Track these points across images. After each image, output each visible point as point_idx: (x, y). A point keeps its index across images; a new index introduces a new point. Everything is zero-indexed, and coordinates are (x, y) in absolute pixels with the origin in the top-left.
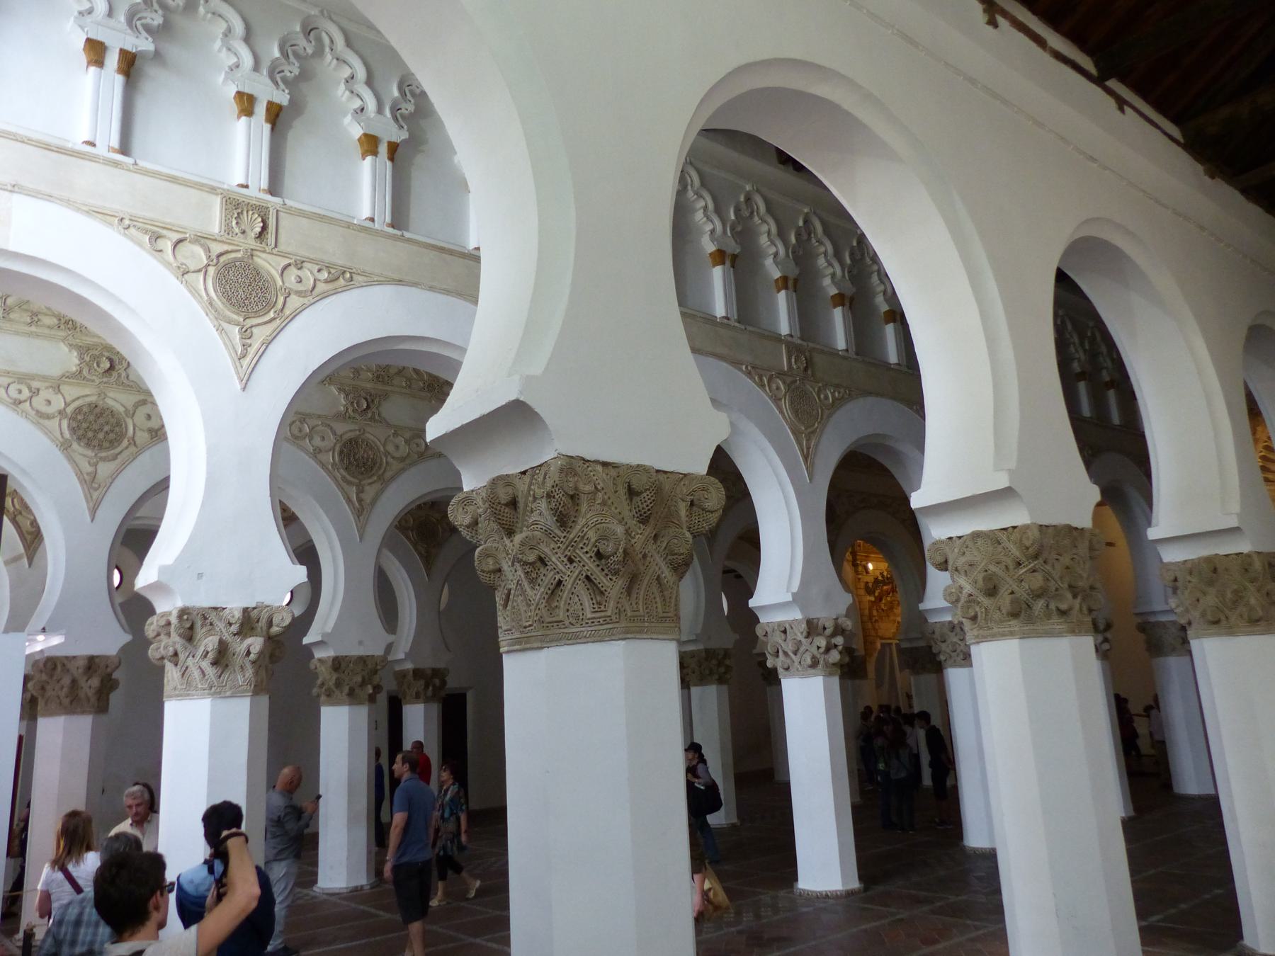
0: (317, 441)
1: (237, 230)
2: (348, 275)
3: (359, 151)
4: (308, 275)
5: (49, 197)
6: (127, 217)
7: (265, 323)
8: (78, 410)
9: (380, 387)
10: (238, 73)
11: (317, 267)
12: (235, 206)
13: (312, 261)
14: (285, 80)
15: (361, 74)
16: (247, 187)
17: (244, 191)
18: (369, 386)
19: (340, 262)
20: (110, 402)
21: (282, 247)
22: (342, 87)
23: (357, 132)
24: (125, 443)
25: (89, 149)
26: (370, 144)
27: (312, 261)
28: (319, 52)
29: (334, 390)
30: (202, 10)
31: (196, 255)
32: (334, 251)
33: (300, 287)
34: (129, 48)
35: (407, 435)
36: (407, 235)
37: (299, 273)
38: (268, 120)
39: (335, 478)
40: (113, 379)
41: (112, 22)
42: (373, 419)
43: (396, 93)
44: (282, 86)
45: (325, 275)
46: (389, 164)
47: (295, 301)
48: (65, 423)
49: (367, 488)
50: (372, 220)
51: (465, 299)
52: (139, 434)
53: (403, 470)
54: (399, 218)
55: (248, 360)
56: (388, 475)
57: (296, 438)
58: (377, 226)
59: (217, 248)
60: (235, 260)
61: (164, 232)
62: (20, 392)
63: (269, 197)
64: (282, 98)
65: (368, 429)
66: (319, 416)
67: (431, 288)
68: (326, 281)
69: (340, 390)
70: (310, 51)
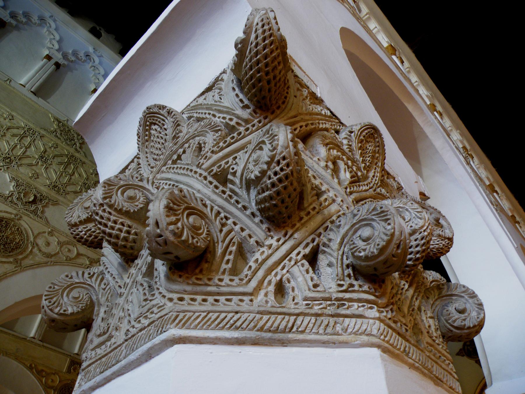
9: (53, 194)
18: (43, 189)
29: (7, 177)
42: (35, 212)
53: (46, 264)
56: (28, 262)
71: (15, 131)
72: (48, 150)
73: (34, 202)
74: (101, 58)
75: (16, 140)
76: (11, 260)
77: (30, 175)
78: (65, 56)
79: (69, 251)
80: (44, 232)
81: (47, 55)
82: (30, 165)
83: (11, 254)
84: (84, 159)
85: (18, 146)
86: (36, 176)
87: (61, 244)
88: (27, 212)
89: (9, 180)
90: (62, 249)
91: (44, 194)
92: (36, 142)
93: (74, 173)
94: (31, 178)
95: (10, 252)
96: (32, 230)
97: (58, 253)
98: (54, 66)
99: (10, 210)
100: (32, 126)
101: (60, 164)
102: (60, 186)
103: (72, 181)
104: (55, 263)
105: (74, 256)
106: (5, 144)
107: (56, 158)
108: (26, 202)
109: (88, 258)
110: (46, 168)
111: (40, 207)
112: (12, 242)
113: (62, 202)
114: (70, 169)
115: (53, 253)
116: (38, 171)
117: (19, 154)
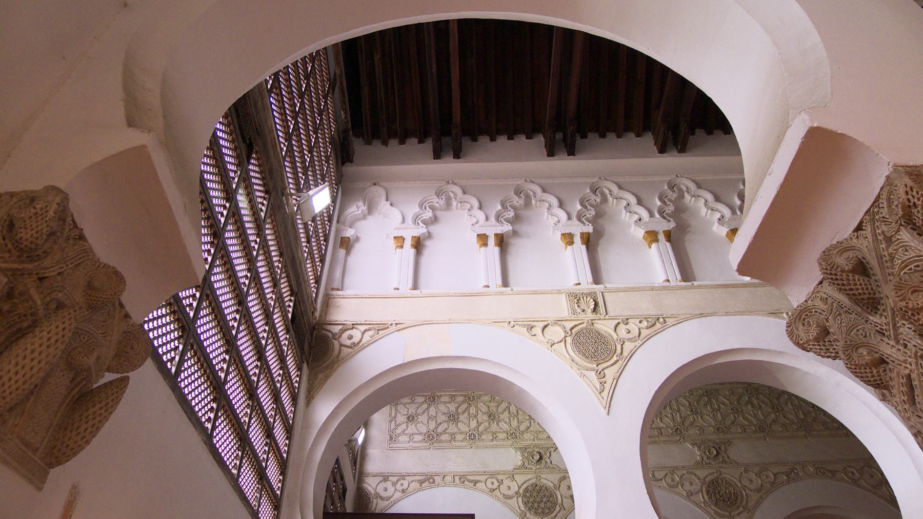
0: (687, 485)
1: (579, 311)
2: (661, 320)
3: (646, 244)
4: (633, 326)
5: (469, 321)
6: (512, 321)
7: (612, 365)
8: (526, 490)
9: (721, 436)
10: (560, 225)
11: (638, 321)
12: (576, 298)
13: (633, 317)
14: (587, 220)
15: (633, 200)
16: (579, 284)
17: (578, 287)
18: (713, 437)
19: (654, 313)
20: (543, 481)
21: (611, 313)
22: (624, 211)
23: (640, 233)
24: (558, 508)
25: (487, 289)
26: (652, 237)
27: (633, 317)
28: (604, 199)
30: (533, 202)
31: (556, 333)
32: (646, 306)
33: (630, 336)
34: (499, 232)
35: (756, 469)
36: (696, 283)
37: (627, 327)
38: (583, 243)
39: (708, 513)
40: (543, 465)
41: (488, 223)
42: (724, 462)
43: (659, 203)
44: (587, 223)
45: (645, 324)
46: (668, 244)
47: (628, 347)
48: (520, 499)
50: (668, 281)
51: (758, 315)
52: (564, 500)
54: (687, 274)
55: (608, 394)
56: (751, 504)
58: (672, 284)
59: (569, 325)
60: (582, 330)
61: (535, 324)
62: (493, 483)
63: (595, 286)
64: (589, 229)
65: (723, 470)
66: (683, 467)
67: (727, 314)
68: (647, 328)
69: (693, 444)
70: (598, 200)
79: (767, 476)
82: (692, 424)
86: (702, 429)
87: (758, 475)
101: (705, 405)
110: (702, 417)
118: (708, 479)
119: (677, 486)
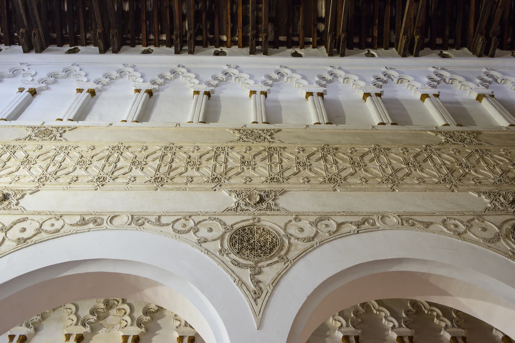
0: (203, 233)
9: (275, 186)
29: (225, 193)
35: (313, 219)
42: (269, 208)
49: (265, 270)
53: (312, 248)
56: (292, 255)
57: (179, 232)
65: (263, 218)
71: (207, 156)
72: (245, 155)
73: (262, 200)
74: (239, 68)
75: (212, 162)
76: (276, 259)
77: (244, 181)
78: (209, 84)
79: (327, 226)
80: (290, 221)
81: (194, 92)
82: (238, 174)
83: (272, 254)
84: (282, 145)
85: (218, 165)
88: (262, 212)
89: (228, 195)
90: (319, 227)
91: (267, 189)
92: (230, 154)
93: (281, 160)
94: (245, 183)
95: (270, 253)
96: (277, 225)
97: (317, 233)
98: (205, 96)
99: (245, 218)
100: (218, 145)
101: (263, 159)
102: (276, 176)
103: (284, 167)
104: (322, 243)
105: (335, 229)
106: (206, 169)
107: (256, 157)
108: (255, 204)
109: (352, 223)
111: (270, 201)
112: (265, 243)
113: (288, 188)
114: (276, 159)
115: (312, 235)
116: (248, 175)
117: (222, 171)
118: (236, 227)
119: (189, 231)
